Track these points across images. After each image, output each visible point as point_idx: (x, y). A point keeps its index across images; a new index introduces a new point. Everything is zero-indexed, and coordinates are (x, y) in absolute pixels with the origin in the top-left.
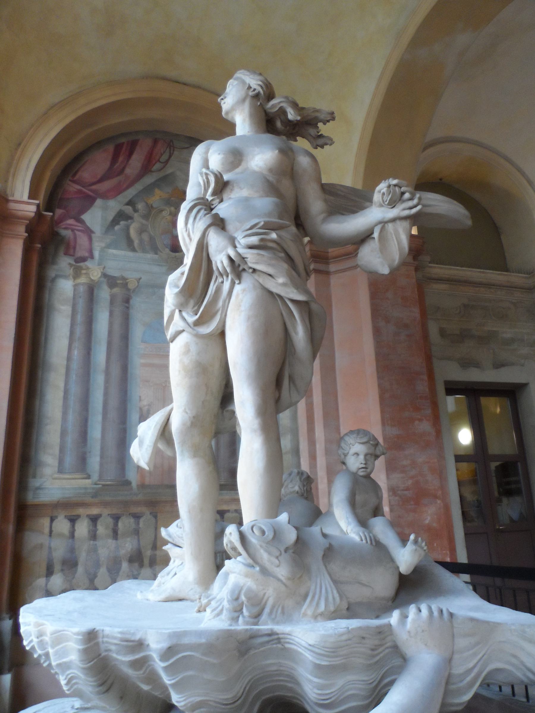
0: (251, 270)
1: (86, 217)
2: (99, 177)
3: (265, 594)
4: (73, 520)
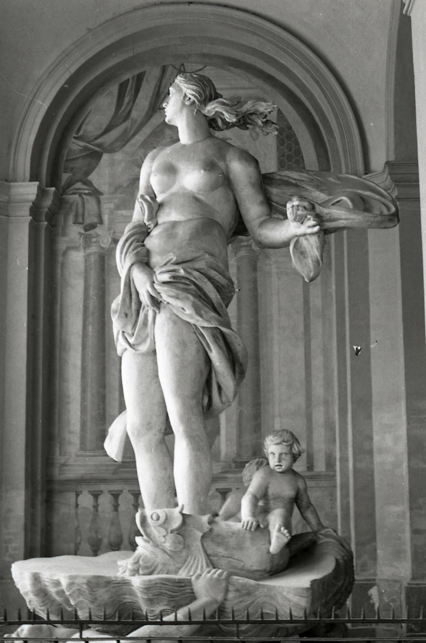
0: (165, 303)
1: (93, 177)
2: (104, 127)
3: (155, 562)
4: (96, 496)
